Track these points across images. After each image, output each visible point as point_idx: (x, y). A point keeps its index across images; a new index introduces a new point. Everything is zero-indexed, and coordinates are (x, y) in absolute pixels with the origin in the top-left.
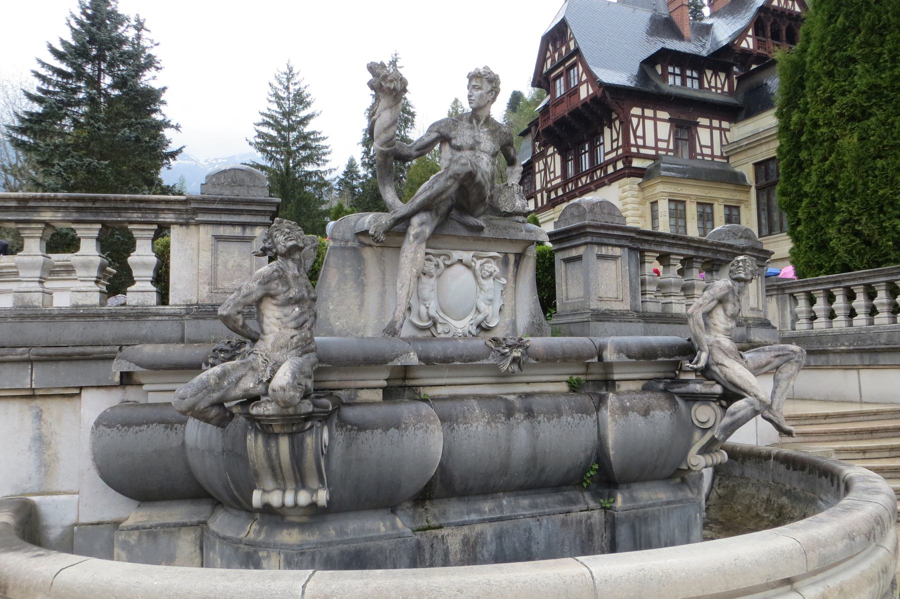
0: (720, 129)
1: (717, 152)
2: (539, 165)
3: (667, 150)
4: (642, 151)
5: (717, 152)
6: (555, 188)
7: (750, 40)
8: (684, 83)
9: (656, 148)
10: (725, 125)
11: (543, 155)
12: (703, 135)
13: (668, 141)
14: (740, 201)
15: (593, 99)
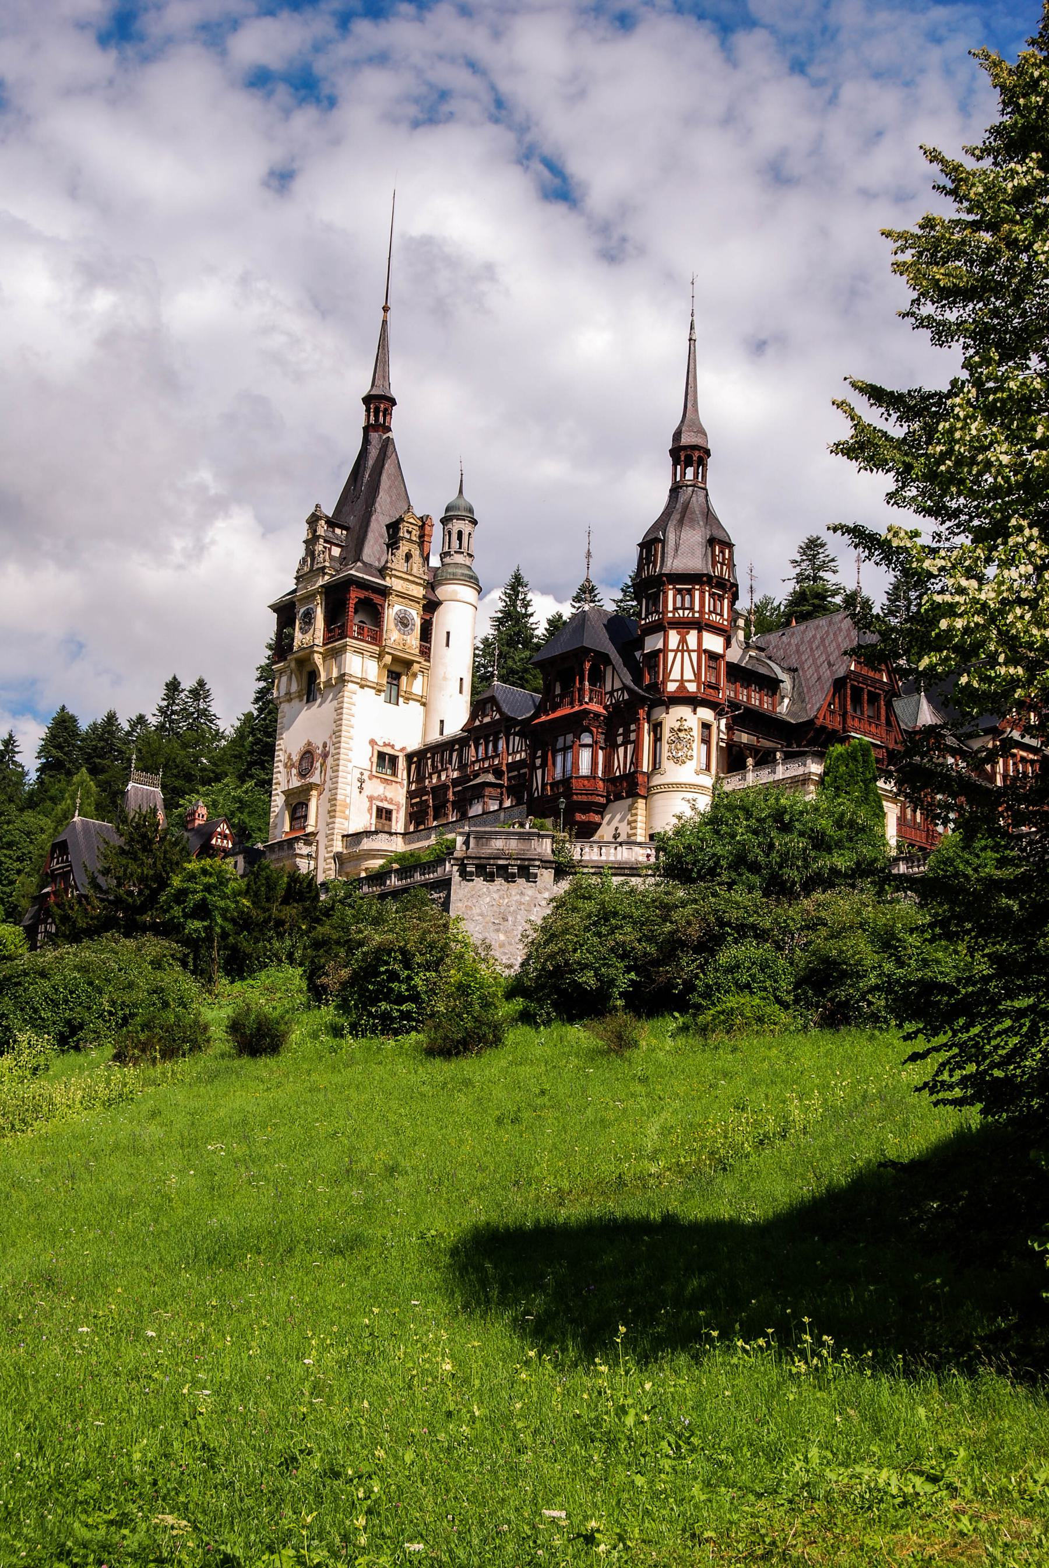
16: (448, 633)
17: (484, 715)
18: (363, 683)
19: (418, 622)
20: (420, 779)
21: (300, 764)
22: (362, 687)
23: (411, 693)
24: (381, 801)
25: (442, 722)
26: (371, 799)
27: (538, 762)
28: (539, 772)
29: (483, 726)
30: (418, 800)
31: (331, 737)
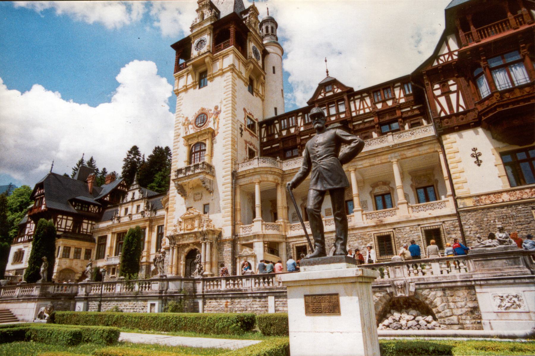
0: (92, 224)
1: (89, 231)
2: (28, 225)
3: (69, 229)
4: (59, 229)
5: (89, 231)
6: (31, 235)
7: (108, 198)
8: (81, 209)
9: (65, 229)
10: (94, 223)
11: (29, 222)
12: (85, 226)
13: (70, 227)
14: (92, 248)
15: (45, 211)
16: (274, 68)
17: (326, 92)
18: (240, 74)
19: (260, 56)
20: (270, 136)
21: (195, 122)
22: (240, 77)
23: (259, 91)
24: (250, 145)
25: (276, 109)
26: (246, 142)
27: (438, 93)
28: (442, 100)
29: (325, 98)
30: (269, 147)
31: (221, 102)
